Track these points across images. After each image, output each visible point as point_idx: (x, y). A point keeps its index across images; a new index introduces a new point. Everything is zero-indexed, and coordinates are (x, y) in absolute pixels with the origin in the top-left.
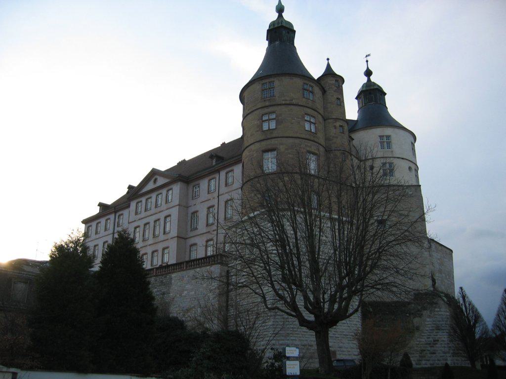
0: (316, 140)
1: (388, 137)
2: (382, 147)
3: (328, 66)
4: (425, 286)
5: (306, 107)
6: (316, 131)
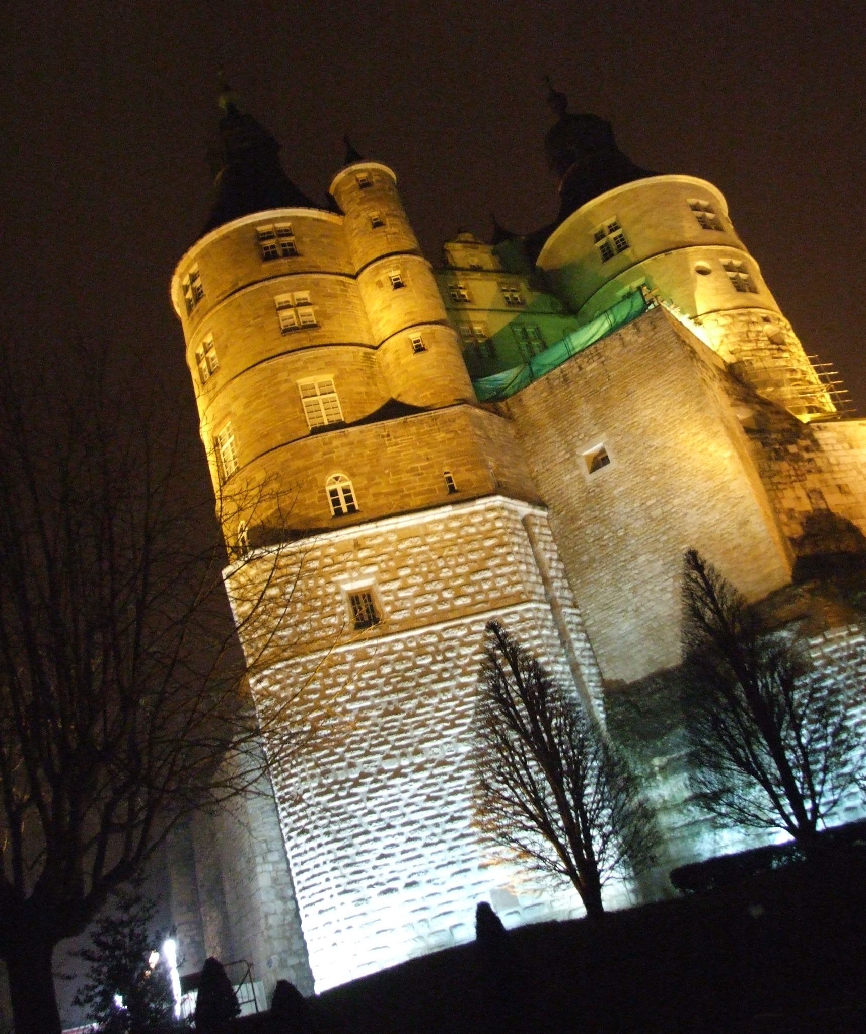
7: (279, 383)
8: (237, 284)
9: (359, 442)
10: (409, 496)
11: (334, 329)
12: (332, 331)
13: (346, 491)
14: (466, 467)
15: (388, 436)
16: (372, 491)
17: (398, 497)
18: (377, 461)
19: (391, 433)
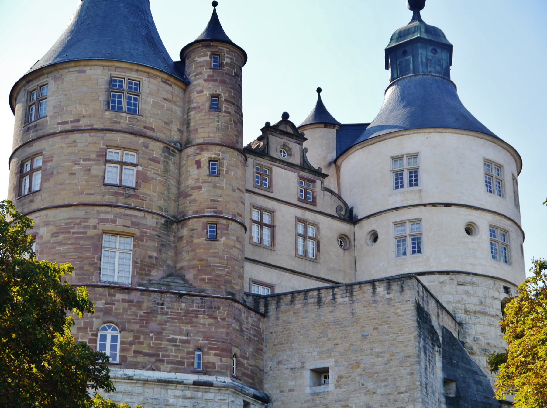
1: (414, 156)
2: (399, 184)
5: (113, 130)
6: (137, 182)
7: (88, 227)
8: (78, 121)
9: (138, 302)
10: (163, 361)
11: (149, 192)
12: (146, 194)
13: (114, 338)
14: (214, 352)
15: (163, 304)
16: (134, 348)
17: (153, 359)
19: (165, 303)
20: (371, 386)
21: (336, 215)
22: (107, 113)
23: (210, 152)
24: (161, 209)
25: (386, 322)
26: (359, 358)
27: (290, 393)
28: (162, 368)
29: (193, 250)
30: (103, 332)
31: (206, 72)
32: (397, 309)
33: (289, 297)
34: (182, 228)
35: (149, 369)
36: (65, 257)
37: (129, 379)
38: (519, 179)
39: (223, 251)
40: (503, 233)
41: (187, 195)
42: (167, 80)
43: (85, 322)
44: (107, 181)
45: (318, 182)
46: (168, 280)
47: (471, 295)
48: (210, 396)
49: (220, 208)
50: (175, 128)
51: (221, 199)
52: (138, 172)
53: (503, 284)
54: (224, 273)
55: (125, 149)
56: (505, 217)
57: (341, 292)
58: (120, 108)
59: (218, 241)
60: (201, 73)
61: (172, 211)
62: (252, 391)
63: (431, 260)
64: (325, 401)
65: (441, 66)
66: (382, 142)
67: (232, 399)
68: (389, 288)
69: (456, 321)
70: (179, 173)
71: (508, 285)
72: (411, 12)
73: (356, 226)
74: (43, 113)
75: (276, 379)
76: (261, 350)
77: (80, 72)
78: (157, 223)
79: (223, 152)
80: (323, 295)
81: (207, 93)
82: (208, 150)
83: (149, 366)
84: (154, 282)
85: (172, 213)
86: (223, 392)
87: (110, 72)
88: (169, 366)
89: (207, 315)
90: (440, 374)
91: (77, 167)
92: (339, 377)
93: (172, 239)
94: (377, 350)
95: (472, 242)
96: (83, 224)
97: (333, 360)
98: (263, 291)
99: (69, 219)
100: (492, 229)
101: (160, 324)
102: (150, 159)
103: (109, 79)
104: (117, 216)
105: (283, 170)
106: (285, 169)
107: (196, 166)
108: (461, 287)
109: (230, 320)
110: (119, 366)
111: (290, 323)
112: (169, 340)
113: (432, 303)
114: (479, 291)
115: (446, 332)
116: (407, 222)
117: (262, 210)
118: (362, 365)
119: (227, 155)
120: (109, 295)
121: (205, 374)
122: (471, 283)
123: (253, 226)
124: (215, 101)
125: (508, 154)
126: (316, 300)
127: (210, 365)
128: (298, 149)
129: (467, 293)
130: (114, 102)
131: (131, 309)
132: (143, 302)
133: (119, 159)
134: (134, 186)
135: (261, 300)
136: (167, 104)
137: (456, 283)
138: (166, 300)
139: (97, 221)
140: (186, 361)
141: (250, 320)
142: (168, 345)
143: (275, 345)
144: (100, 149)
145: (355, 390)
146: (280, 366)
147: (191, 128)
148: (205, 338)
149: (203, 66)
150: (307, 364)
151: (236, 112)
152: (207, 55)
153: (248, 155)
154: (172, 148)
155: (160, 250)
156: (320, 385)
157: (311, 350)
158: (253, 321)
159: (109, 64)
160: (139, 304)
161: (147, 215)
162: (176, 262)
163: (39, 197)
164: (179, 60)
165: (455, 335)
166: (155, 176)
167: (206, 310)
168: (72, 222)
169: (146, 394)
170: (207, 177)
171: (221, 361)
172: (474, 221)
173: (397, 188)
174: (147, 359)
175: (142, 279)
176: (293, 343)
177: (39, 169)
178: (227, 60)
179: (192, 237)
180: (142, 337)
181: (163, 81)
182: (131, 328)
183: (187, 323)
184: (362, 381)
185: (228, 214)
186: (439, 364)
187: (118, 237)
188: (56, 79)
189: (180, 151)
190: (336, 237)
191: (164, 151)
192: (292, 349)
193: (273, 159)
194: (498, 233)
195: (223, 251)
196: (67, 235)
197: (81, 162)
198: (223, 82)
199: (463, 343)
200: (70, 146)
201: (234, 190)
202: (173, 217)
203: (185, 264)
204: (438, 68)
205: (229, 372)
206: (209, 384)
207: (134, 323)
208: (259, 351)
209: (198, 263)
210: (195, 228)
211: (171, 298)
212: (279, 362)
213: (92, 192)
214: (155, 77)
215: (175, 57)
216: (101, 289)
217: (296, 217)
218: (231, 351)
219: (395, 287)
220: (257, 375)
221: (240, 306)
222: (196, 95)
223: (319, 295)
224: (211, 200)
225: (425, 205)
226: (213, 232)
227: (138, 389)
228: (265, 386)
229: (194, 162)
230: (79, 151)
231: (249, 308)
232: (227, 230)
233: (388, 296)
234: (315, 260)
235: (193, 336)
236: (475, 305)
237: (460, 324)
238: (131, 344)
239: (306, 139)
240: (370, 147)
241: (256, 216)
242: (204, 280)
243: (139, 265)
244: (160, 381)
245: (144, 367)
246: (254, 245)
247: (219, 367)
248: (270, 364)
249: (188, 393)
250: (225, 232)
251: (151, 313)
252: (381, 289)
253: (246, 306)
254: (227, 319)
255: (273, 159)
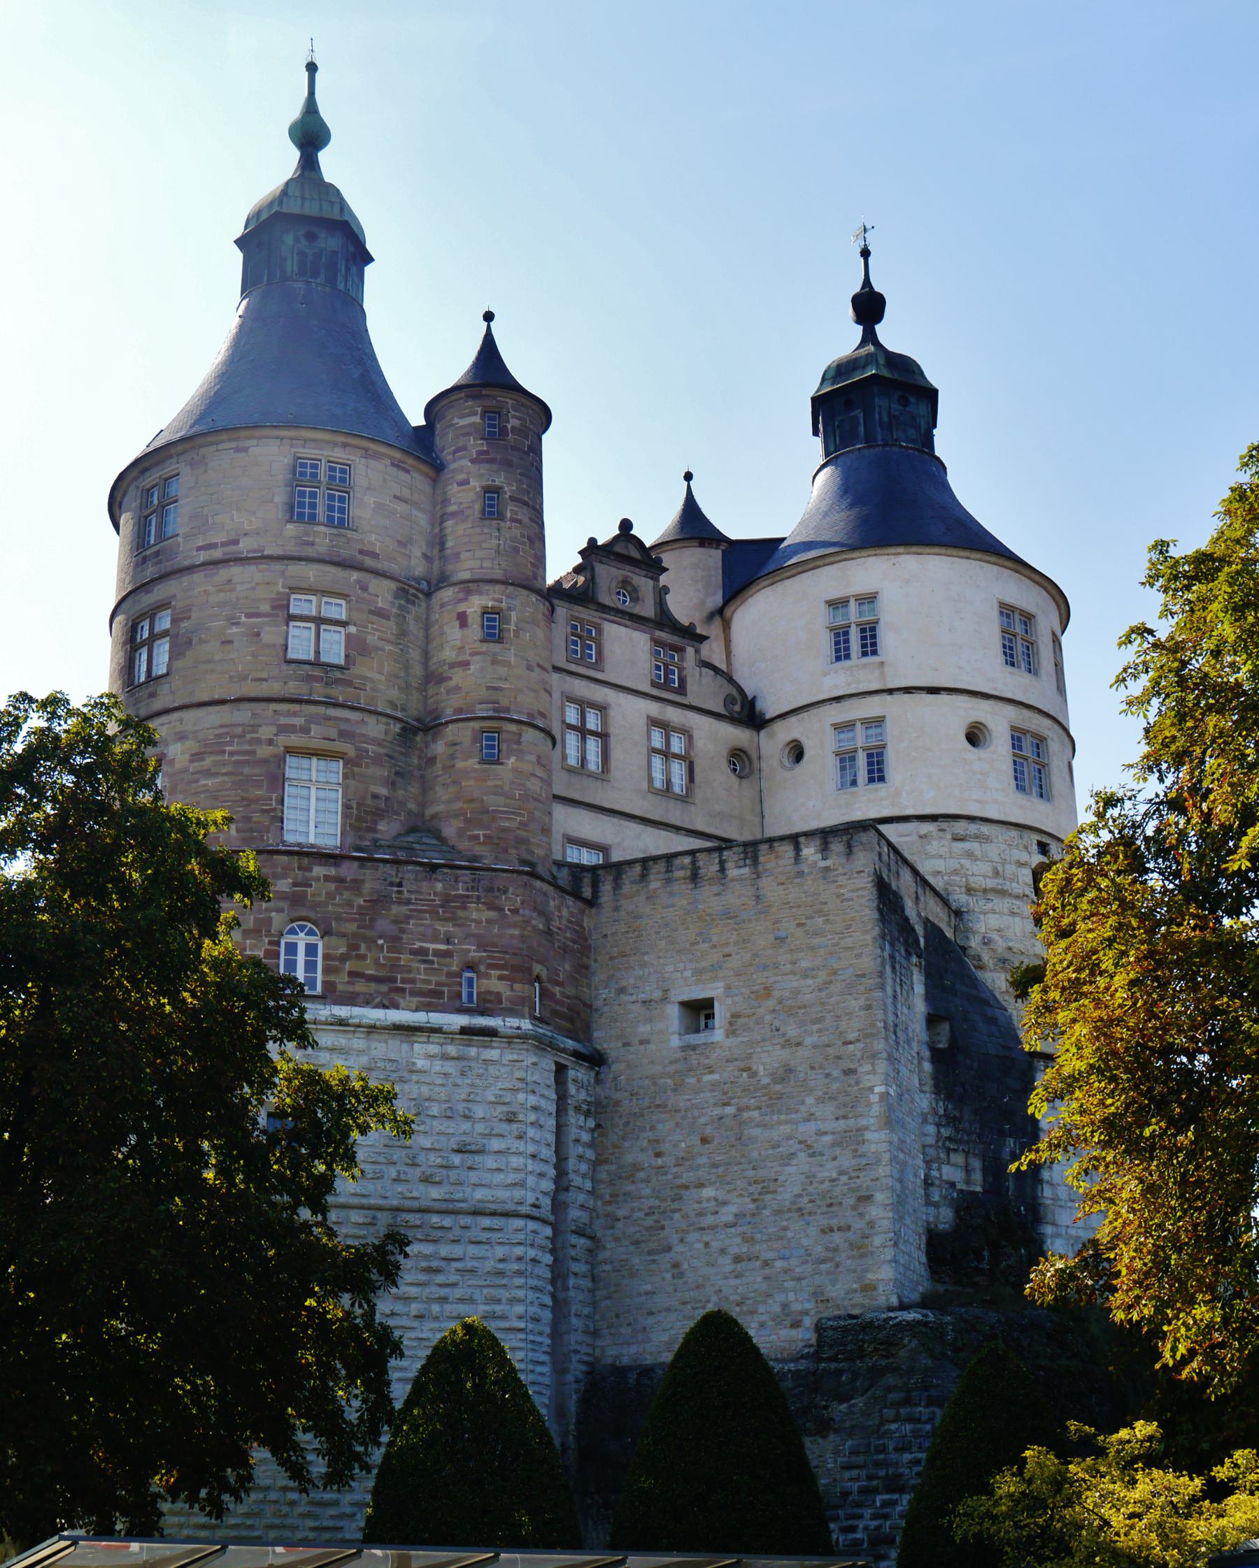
0: (340, 694)
1: (869, 599)
2: (841, 653)
3: (489, 348)
4: (869, 1288)
5: (300, 559)
6: (347, 656)
7: (258, 741)
8: (236, 542)
9: (355, 881)
10: (402, 990)
13: (311, 950)
14: (498, 972)
15: (400, 885)
16: (348, 966)
17: (384, 988)
18: (371, 920)
19: (405, 882)
20: (792, 1031)
21: (723, 712)
22: (290, 526)
23: (484, 597)
24: (392, 704)
25: (820, 912)
26: (771, 980)
27: (642, 1047)
28: (402, 1003)
29: (454, 783)
30: (291, 938)
31: (475, 445)
32: (840, 886)
33: (638, 869)
34: (434, 740)
35: (376, 1007)
36: (215, 798)
37: (341, 1025)
38: (1065, 640)
39: (512, 783)
40: (1036, 741)
41: (442, 679)
42: (400, 461)
43: (256, 920)
44: (292, 655)
45: (690, 651)
46: (410, 839)
47: (977, 859)
48: (493, 1054)
49: (504, 703)
50: (417, 551)
51: (506, 685)
52: (348, 636)
53: (1036, 837)
54: (514, 825)
55: (325, 593)
56: (1040, 711)
57: (736, 857)
58: (313, 517)
59: (502, 764)
60: (464, 448)
61: (414, 706)
62: (570, 1044)
63: (904, 794)
64: (707, 1061)
65: (918, 428)
66: (809, 573)
67: (534, 1059)
68: (825, 849)
69: (949, 908)
70: (427, 637)
71: (1045, 840)
72: (859, 329)
73: (763, 733)
74: (170, 530)
75: (616, 1021)
76: (587, 968)
77: (237, 450)
78: (386, 733)
79: (508, 597)
80: (701, 864)
81: (476, 484)
82: (480, 593)
83: (377, 1000)
84: (383, 843)
85: (415, 713)
86: (517, 1046)
87: (293, 450)
88: (415, 999)
89: (484, 904)
90: (920, 1007)
91: (234, 630)
92: (733, 1016)
93: (416, 761)
94: (804, 964)
95: (980, 759)
96: (248, 736)
97: (721, 984)
98: (587, 858)
99: (222, 726)
100: (1016, 734)
101: (396, 922)
102: (371, 612)
103: (292, 462)
104: (312, 719)
105: (622, 628)
106: (626, 626)
107: (457, 624)
108: (960, 845)
109: (527, 912)
110: (321, 1001)
111: (640, 917)
112: (414, 952)
113: (907, 876)
114: (993, 851)
115: (932, 930)
116: (858, 724)
117: (583, 705)
118: (776, 994)
119: (516, 602)
120: (300, 868)
121: (483, 1013)
122: (977, 837)
123: (568, 736)
124: (491, 499)
125: (1044, 593)
126: (688, 873)
127: (492, 998)
128: (651, 588)
129: (970, 855)
130: (301, 505)
131: (341, 894)
132: (363, 881)
133: (314, 613)
134: (342, 662)
135: (586, 874)
136: (400, 507)
137: (949, 836)
138: (407, 876)
139: (273, 730)
140: (446, 989)
141: (565, 913)
142: (411, 960)
143: (612, 958)
144: (278, 593)
145: (764, 1040)
146: (624, 998)
147: (448, 552)
148: (481, 947)
149: (468, 434)
150: (672, 992)
151: (531, 519)
152: (476, 414)
153: (556, 602)
154: (412, 591)
155: (393, 783)
156: (697, 1031)
157: (681, 966)
158: (572, 914)
159: (292, 433)
160: (356, 886)
161: (367, 717)
162: (423, 805)
163: (166, 686)
164: (423, 423)
165: (949, 934)
166: (380, 644)
167: (481, 894)
168: (227, 733)
169: (374, 1052)
170: (478, 645)
171: (512, 990)
172: (983, 720)
173: (838, 659)
174: (373, 986)
175: (361, 838)
176: (647, 953)
177: (165, 633)
178: (513, 423)
179: (452, 757)
180: (363, 946)
181: (393, 464)
182: (342, 930)
183: (446, 920)
184: (776, 1023)
185: (520, 713)
186: (919, 989)
187: (314, 759)
188: (193, 464)
189: (428, 595)
190: (725, 753)
191: (396, 597)
192: (644, 965)
193: (604, 608)
194: (1027, 743)
195: (512, 783)
196: (219, 758)
197: (243, 619)
198: (507, 464)
199: (964, 949)
200: (221, 591)
201: (530, 668)
202: (417, 720)
203: (440, 808)
204: (912, 432)
205: (526, 1010)
206: (491, 1033)
207: (347, 920)
208: (582, 970)
209: (465, 806)
210: (458, 740)
211: (416, 872)
212: (622, 990)
213: (265, 675)
214: (377, 456)
215: (416, 419)
216: (285, 858)
217: (648, 717)
218: (529, 970)
219: (837, 846)
220: (578, 1013)
221: (546, 887)
222: (456, 488)
223: (694, 863)
224: (488, 688)
225: (891, 691)
226: (492, 747)
227: (358, 1043)
228: (596, 1034)
229: (455, 615)
230: (238, 599)
231: (563, 890)
232: (519, 743)
233: (823, 864)
234: (685, 799)
235: (459, 943)
236: (985, 877)
237: (958, 913)
238: (343, 958)
239: (666, 570)
240: (787, 582)
241: (572, 716)
242: (477, 837)
243: (355, 811)
244: (398, 1028)
245: (367, 1003)
246: (570, 770)
247: (508, 1000)
248: (604, 993)
249: (452, 1050)
250: (515, 746)
251: (379, 902)
252: (810, 851)
253: (556, 887)
254: (521, 911)
255: (604, 608)
